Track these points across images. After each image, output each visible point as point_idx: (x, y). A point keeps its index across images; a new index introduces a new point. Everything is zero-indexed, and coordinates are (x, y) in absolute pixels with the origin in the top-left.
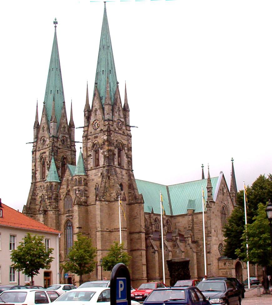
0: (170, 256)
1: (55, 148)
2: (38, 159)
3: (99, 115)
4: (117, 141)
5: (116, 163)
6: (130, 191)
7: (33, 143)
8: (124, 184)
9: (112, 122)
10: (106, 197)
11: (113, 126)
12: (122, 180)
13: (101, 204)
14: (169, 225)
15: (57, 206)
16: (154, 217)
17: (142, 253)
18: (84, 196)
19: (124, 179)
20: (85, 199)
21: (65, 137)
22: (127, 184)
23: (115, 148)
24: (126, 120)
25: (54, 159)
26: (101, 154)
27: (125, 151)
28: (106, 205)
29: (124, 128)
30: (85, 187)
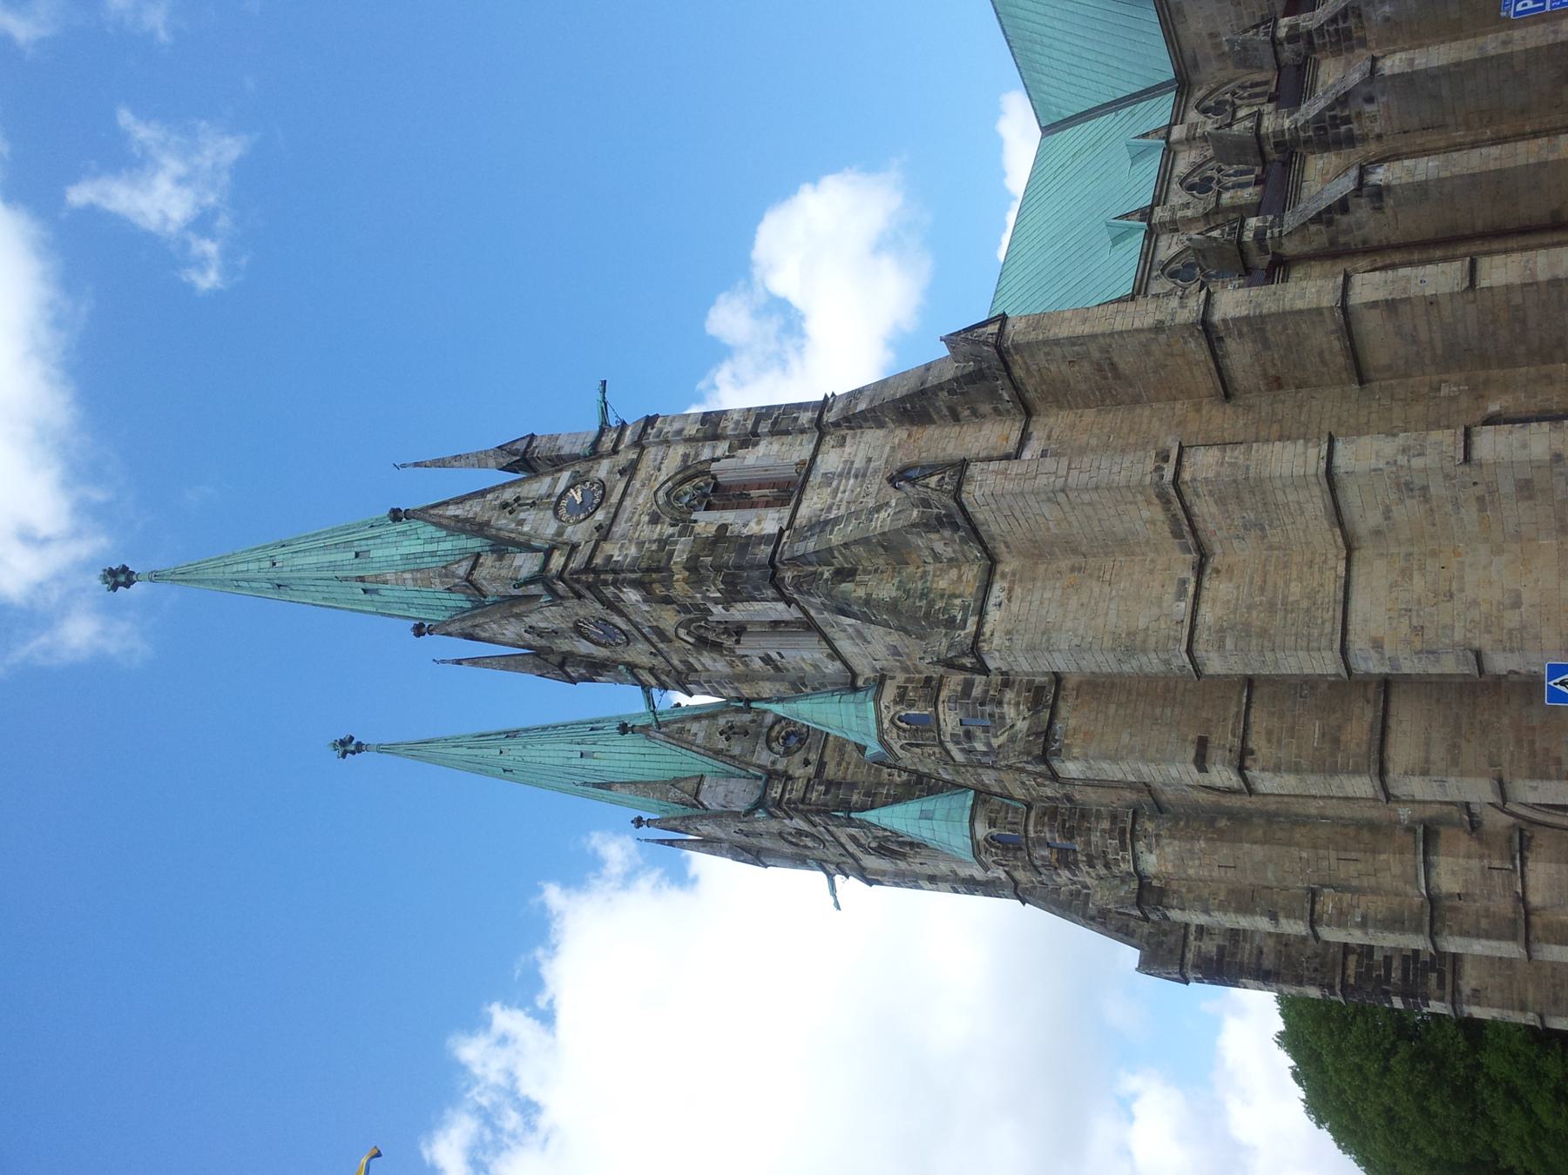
0: (1411, 61)
1: (814, 796)
2: (896, 864)
3: (546, 619)
4: (655, 519)
5: (769, 522)
6: (945, 411)
7: (830, 877)
8: (902, 459)
9: (556, 554)
10: (958, 602)
11: (574, 548)
12: (875, 472)
13: (996, 641)
14: (1234, 94)
15: (1106, 825)
16: (1177, 196)
17: (1374, 305)
18: (1000, 703)
19: (869, 460)
20: (1018, 704)
21: (772, 728)
22: (901, 434)
23: (686, 526)
24: (575, 458)
25: (863, 809)
26: (732, 610)
27: (718, 460)
28: (1009, 600)
29: (603, 470)
30: (944, 694)
